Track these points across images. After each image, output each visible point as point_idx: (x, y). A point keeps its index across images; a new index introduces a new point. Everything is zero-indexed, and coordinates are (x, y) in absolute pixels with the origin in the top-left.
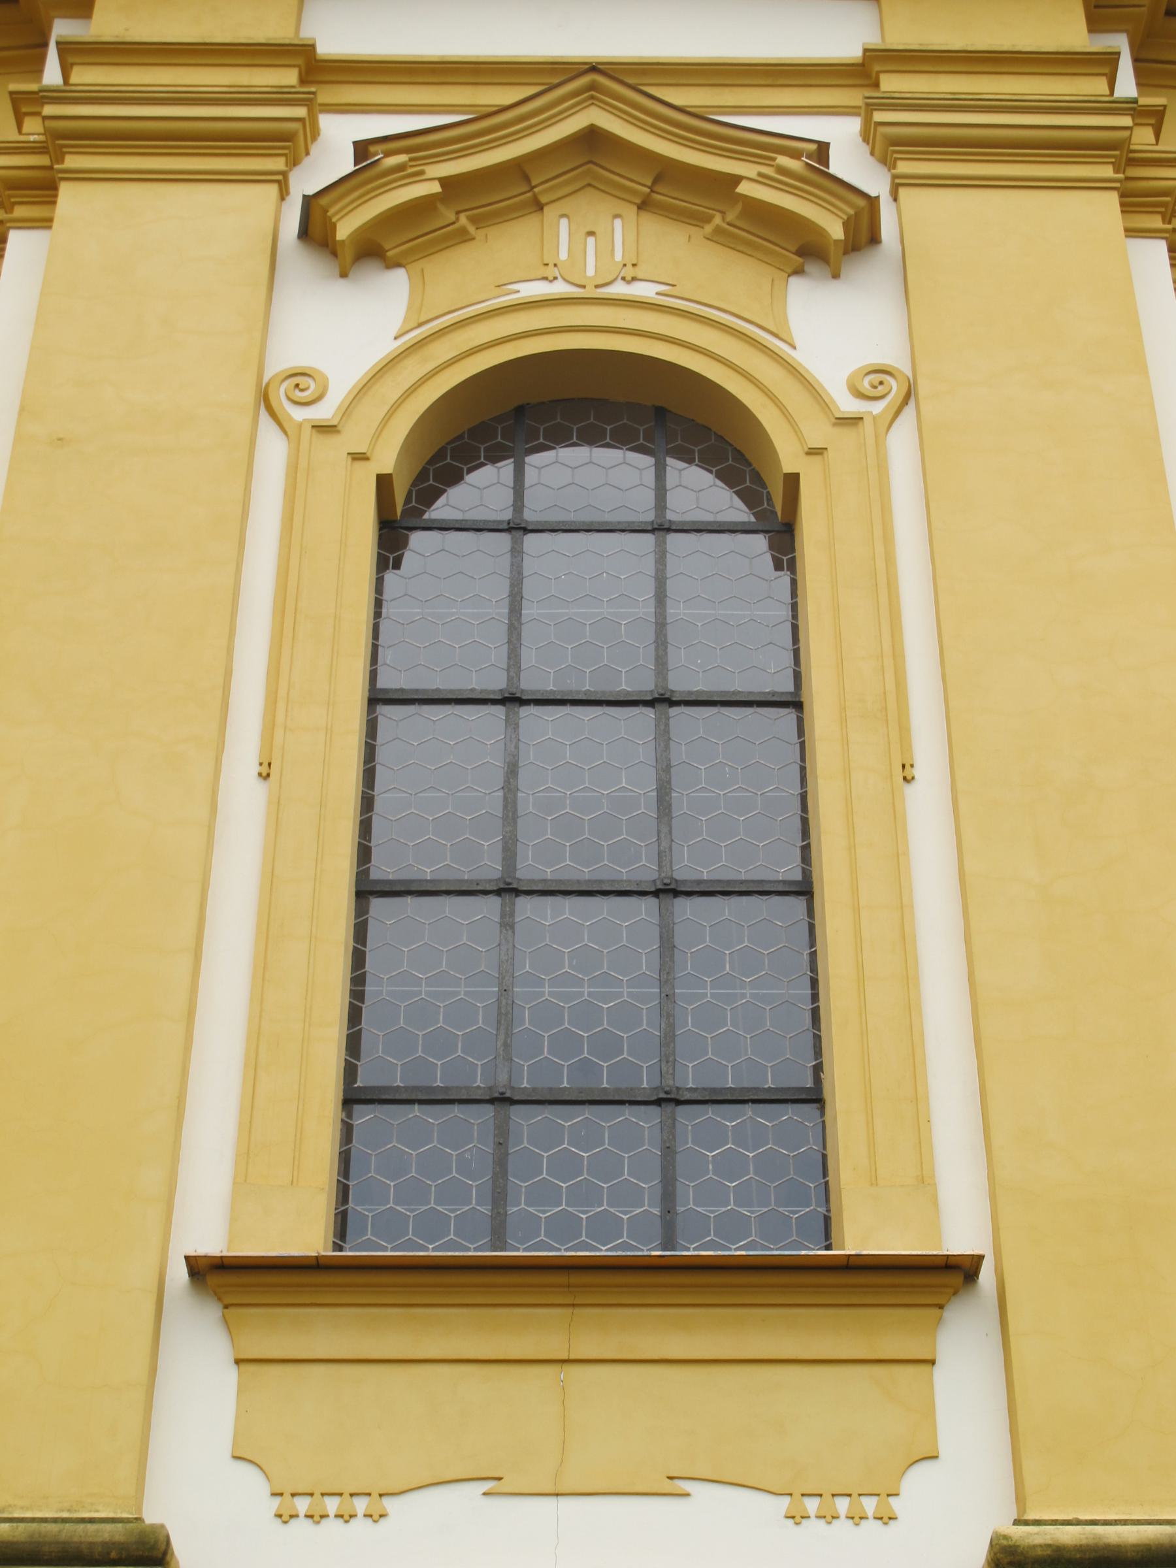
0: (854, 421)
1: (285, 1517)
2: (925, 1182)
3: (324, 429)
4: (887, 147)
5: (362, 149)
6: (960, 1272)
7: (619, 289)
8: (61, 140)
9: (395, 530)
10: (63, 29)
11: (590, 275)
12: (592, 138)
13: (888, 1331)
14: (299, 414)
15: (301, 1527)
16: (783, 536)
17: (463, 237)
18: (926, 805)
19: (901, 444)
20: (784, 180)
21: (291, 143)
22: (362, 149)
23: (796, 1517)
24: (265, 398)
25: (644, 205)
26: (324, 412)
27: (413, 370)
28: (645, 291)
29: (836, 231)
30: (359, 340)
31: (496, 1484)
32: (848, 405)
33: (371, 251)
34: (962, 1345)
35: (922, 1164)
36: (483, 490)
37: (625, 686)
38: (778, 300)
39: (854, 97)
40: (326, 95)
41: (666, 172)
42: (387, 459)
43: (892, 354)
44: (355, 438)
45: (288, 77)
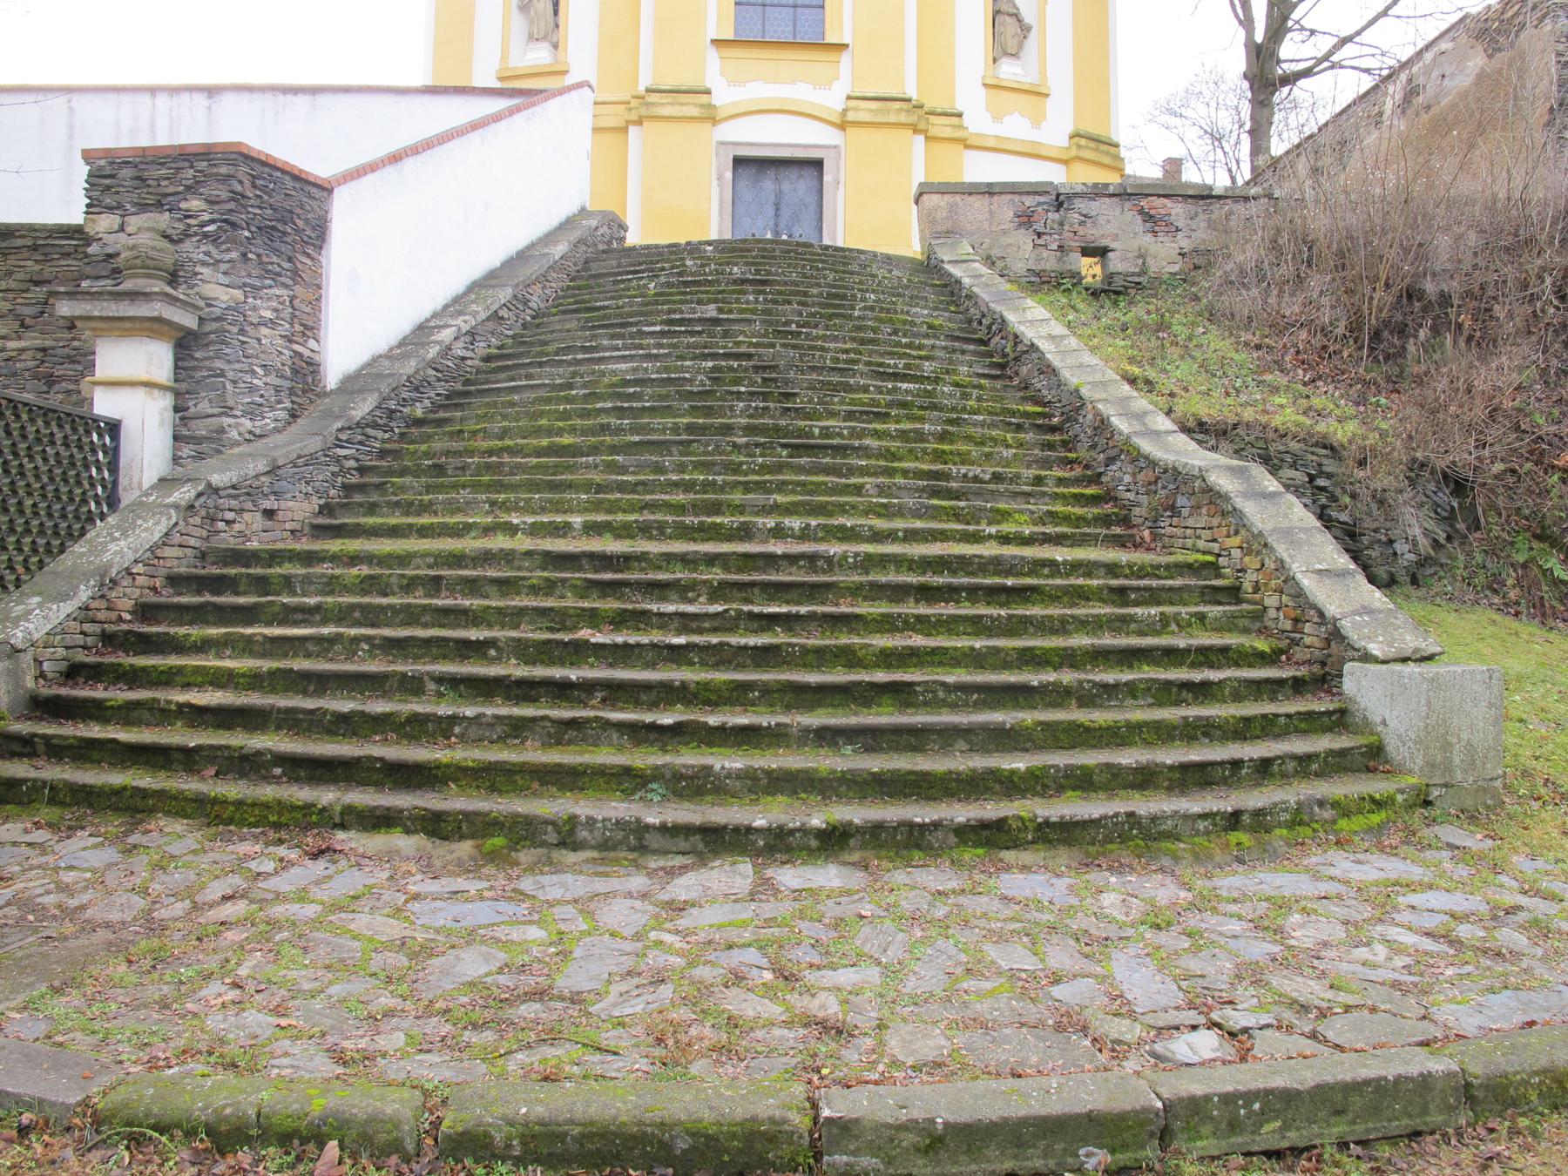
2: (841, 27)
13: (832, 56)
34: (845, 58)
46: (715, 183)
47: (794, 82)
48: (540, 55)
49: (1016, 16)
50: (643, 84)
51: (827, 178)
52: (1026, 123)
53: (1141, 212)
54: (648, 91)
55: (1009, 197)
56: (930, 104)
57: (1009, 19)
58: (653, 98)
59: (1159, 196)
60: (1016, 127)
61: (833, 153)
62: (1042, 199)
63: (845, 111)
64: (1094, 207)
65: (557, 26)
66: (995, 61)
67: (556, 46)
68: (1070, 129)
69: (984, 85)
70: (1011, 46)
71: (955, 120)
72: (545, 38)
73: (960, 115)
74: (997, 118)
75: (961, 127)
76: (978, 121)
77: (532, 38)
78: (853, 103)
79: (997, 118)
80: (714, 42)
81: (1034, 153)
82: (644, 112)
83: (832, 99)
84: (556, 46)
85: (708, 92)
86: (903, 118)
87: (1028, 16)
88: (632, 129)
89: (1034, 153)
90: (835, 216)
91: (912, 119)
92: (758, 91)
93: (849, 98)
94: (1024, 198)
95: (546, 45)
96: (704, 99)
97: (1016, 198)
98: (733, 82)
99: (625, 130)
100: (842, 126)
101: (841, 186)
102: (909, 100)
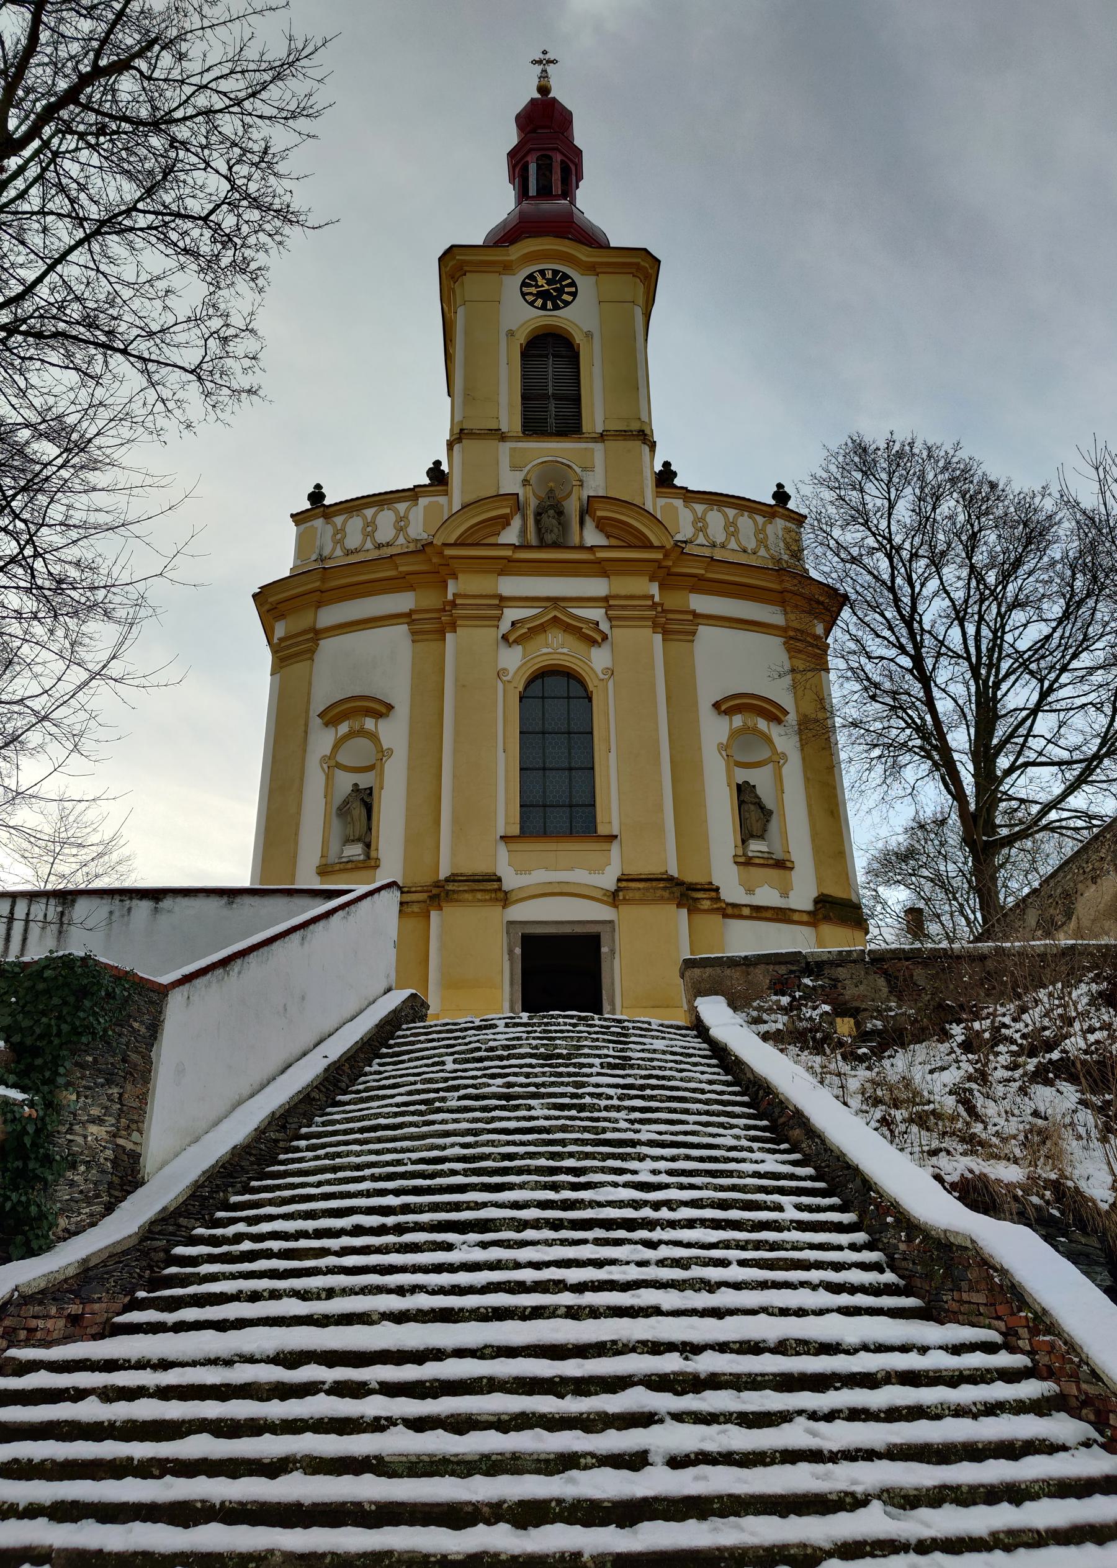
4: (610, 619)
6: (616, 837)
7: (560, 650)
9: (521, 699)
10: (452, 588)
11: (556, 648)
13: (605, 846)
14: (504, 678)
16: (590, 700)
18: (613, 756)
19: (611, 684)
21: (499, 618)
22: (513, 624)
26: (508, 678)
27: (524, 669)
28: (565, 650)
30: (514, 661)
31: (547, 869)
32: (602, 676)
33: (515, 641)
34: (615, 847)
38: (589, 652)
39: (605, 604)
40: (503, 604)
42: (521, 688)
43: (610, 665)
44: (514, 684)
46: (506, 957)
47: (572, 869)
50: (443, 873)
51: (604, 950)
52: (776, 893)
54: (447, 880)
56: (690, 878)
57: (752, 807)
60: (767, 896)
61: (608, 928)
63: (619, 889)
65: (370, 829)
66: (743, 842)
68: (814, 894)
69: (735, 863)
70: (756, 828)
71: (713, 894)
72: (359, 840)
73: (717, 890)
74: (750, 891)
75: (718, 899)
76: (732, 891)
77: (348, 841)
78: (624, 884)
79: (750, 891)
81: (782, 915)
83: (608, 880)
84: (368, 846)
85: (499, 880)
87: (769, 802)
89: (782, 915)
90: (613, 984)
92: (540, 876)
93: (619, 880)
96: (495, 885)
101: (617, 955)
102: (671, 879)
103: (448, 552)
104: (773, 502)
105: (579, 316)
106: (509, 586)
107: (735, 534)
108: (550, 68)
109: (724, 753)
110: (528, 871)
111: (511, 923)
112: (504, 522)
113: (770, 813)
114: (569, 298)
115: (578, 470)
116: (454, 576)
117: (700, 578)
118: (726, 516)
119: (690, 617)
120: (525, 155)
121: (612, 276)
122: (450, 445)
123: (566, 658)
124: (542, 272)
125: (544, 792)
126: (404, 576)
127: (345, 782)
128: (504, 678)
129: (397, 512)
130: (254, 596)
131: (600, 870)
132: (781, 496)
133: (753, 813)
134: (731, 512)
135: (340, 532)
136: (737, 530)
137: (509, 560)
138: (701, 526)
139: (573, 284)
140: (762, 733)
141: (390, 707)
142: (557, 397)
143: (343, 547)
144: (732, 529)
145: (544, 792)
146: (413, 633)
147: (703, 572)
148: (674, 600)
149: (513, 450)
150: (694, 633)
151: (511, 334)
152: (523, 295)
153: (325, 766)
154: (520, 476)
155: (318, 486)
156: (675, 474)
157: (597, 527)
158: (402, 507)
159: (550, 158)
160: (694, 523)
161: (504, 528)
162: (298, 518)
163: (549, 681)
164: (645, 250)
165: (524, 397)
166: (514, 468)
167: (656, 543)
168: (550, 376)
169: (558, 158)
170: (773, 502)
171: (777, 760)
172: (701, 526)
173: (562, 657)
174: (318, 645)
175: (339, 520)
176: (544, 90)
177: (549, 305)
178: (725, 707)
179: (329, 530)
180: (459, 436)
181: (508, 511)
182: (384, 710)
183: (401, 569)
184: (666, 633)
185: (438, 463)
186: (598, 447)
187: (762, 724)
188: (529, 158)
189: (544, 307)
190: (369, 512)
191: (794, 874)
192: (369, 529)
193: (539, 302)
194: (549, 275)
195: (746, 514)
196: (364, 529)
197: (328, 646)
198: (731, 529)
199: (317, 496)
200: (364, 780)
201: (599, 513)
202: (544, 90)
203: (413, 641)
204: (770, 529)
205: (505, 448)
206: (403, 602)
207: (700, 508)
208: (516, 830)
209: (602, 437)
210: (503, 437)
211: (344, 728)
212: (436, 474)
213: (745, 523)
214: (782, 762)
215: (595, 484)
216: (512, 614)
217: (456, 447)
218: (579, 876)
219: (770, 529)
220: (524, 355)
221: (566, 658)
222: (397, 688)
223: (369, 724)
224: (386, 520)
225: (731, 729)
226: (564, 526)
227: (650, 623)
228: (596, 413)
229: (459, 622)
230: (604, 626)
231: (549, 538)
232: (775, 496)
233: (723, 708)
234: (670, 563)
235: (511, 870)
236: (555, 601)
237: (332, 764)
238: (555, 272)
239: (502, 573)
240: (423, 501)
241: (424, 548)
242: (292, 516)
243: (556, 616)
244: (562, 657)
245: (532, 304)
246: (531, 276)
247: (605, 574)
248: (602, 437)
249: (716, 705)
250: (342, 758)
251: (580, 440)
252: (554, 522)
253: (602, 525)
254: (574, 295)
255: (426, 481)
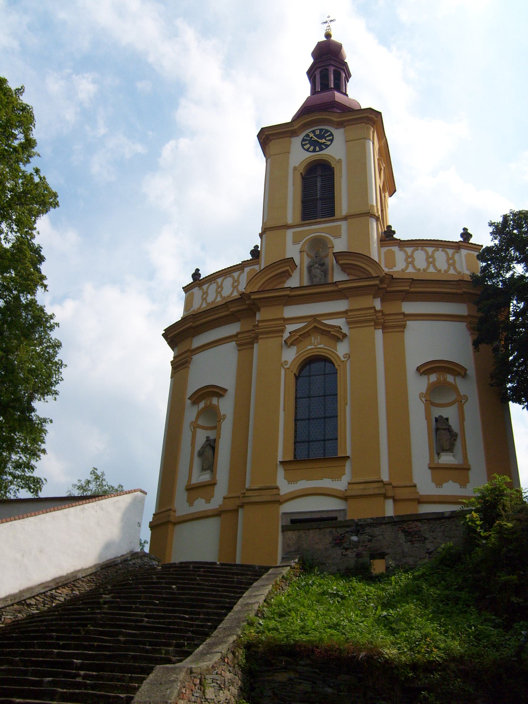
0: (343, 361)
1: (289, 484)
3: (288, 368)
4: (348, 323)
5: (290, 333)
6: (348, 457)
7: (319, 346)
8: (258, 334)
9: (297, 378)
11: (316, 345)
12: (315, 327)
15: (290, 485)
17: (302, 341)
18: (348, 408)
19: (348, 364)
20: (336, 331)
21: (282, 331)
23: (333, 481)
24: (282, 365)
25: (322, 334)
28: (322, 346)
29: (341, 338)
32: (343, 359)
33: (292, 344)
34: (348, 464)
35: (347, 446)
36: (305, 372)
37: (321, 394)
40: (286, 323)
41: (323, 330)
45: (282, 322)
48: (206, 477)
49: (449, 429)
50: (247, 486)
53: (404, 531)
55: (330, 529)
58: (248, 494)
59: (413, 521)
62: (348, 529)
64: (377, 531)
67: (212, 471)
69: (429, 468)
78: (351, 486)
80: (281, 462)
82: (246, 500)
84: (212, 471)
85: (277, 488)
86: (377, 491)
88: (240, 511)
91: (382, 491)
92: (303, 485)
94: (338, 530)
95: (209, 472)
96: (275, 492)
97: (334, 530)
98: (290, 481)
99: (236, 511)
100: (345, 498)
102: (382, 481)
103: (252, 297)
104: (461, 239)
105: (336, 151)
106: (290, 312)
107: (433, 263)
108: (332, 24)
109: (424, 399)
110: (295, 481)
111: (284, 514)
112: (287, 275)
113: (456, 435)
114: (329, 143)
115: (332, 238)
116: (259, 310)
117: (407, 292)
118: (427, 252)
119: (402, 317)
120: (315, 70)
121: (352, 126)
122: (261, 235)
123: (322, 350)
124: (314, 132)
125: (309, 433)
126: (233, 314)
127: (202, 436)
128: (286, 367)
129: (233, 277)
130: (163, 335)
131: (337, 477)
132: (466, 235)
133: (444, 436)
134: (430, 250)
135: (206, 293)
136: (434, 260)
137: (289, 296)
138: (410, 260)
139: (331, 135)
140: (450, 384)
141: (225, 390)
142: (321, 199)
143: (206, 302)
144: (430, 260)
145: (309, 433)
146: (239, 345)
147: (408, 288)
148: (391, 308)
149: (294, 233)
150: (404, 326)
151: (295, 169)
152: (303, 145)
153: (192, 427)
154: (298, 247)
155: (198, 270)
156: (394, 232)
157: (342, 270)
158: (236, 275)
159: (328, 70)
160: (406, 259)
161: (288, 279)
162: (186, 289)
163: (313, 366)
164: (370, 108)
165: (304, 202)
166: (295, 242)
167: (374, 275)
168: (319, 188)
169: (332, 69)
170: (461, 239)
171: (460, 401)
172: (410, 260)
173: (319, 350)
174: (191, 359)
175: (205, 287)
176: (328, 36)
177: (317, 149)
178: (426, 369)
179: (201, 292)
180: (265, 231)
181: (288, 268)
182: (221, 393)
183: (231, 310)
184: (384, 328)
185: (257, 247)
186: (343, 225)
187: (450, 378)
188: (316, 73)
189: (314, 151)
190: (219, 280)
191: (471, 474)
192: (219, 289)
193: (312, 148)
194: (318, 132)
195: (440, 249)
196: (217, 290)
197: (197, 358)
198: (431, 260)
199: (196, 275)
200: (212, 435)
201: (341, 262)
202: (328, 36)
203: (239, 350)
204: (457, 257)
205: (290, 233)
206: (232, 329)
207: (409, 250)
208: (290, 458)
209: (345, 218)
210: (287, 227)
211: (202, 405)
212: (255, 253)
213: (440, 256)
214: (463, 401)
215: (340, 245)
216: (291, 328)
217: (264, 236)
218: (326, 483)
219: (457, 257)
220: (304, 178)
221: (322, 350)
222: (227, 379)
223: (215, 401)
224: (228, 283)
225: (428, 384)
226: (325, 273)
227: (373, 324)
228: (343, 204)
229: (260, 337)
230: (345, 330)
231: (316, 281)
232: (462, 235)
233: (421, 371)
234: (386, 286)
235: (286, 482)
236: (314, 317)
237: (195, 426)
238: (321, 130)
239: (286, 304)
240: (247, 270)
241: (243, 296)
242: (183, 288)
243: (316, 327)
244: (319, 350)
245: (307, 150)
246: (307, 135)
247: (346, 297)
248: (345, 218)
249: (418, 369)
250: (200, 422)
251: (333, 221)
252: (318, 271)
253: (344, 268)
254: (331, 141)
255: (249, 257)
